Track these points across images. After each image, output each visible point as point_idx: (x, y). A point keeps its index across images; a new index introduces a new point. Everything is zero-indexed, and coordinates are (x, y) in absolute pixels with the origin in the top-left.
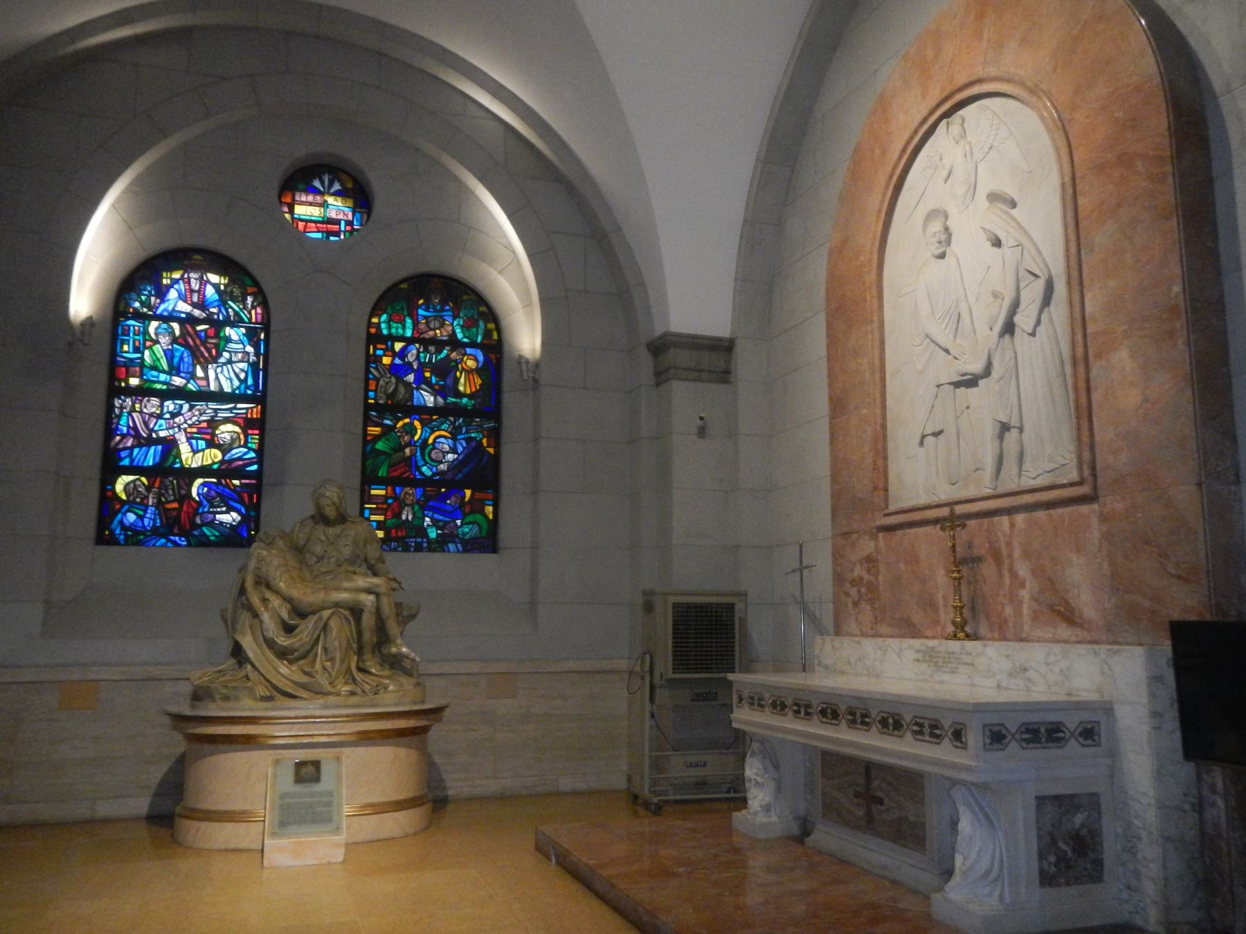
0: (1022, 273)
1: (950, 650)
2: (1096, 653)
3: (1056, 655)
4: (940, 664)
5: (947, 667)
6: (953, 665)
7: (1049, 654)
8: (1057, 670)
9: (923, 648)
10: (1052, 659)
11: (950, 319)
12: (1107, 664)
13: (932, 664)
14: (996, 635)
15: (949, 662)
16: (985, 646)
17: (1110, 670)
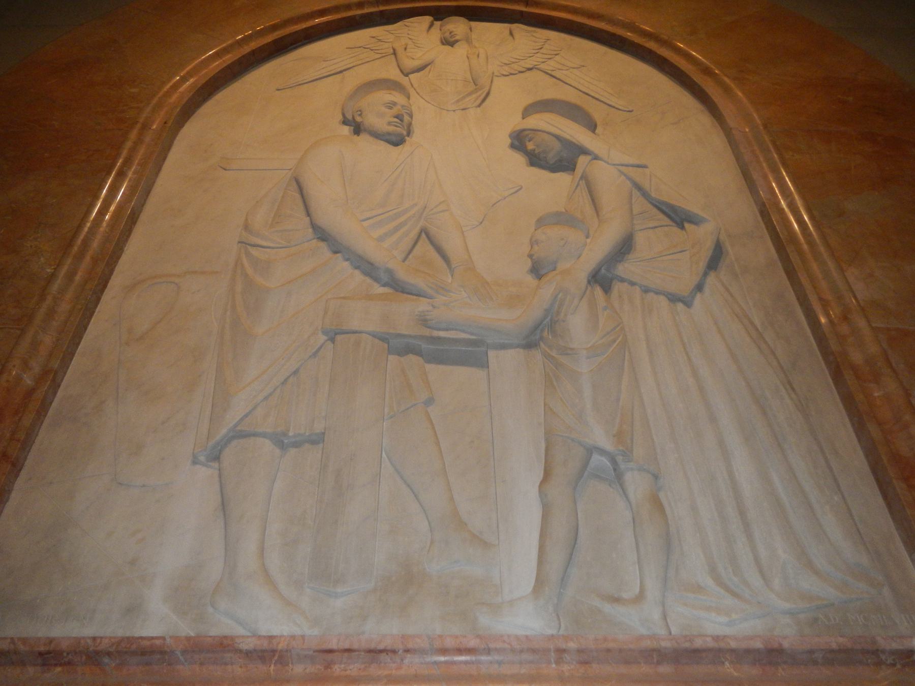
0: (639, 204)
11: (396, 229)
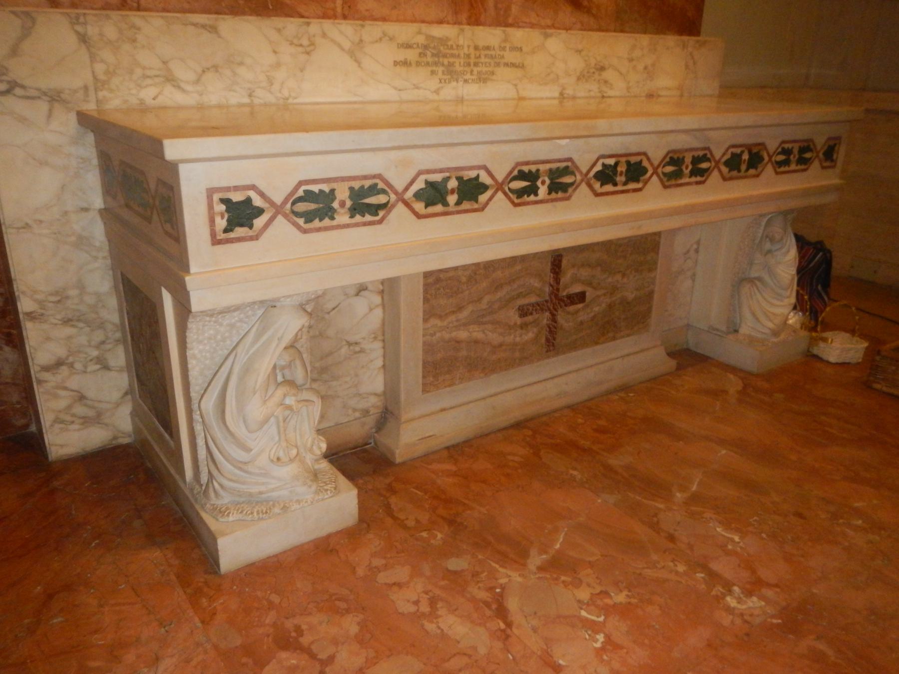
1: (481, 44)
2: (684, 46)
3: (642, 49)
4: (458, 68)
5: (472, 72)
6: (484, 69)
7: (633, 47)
8: (640, 67)
9: (421, 39)
10: (637, 53)
12: (693, 58)
13: (440, 69)
14: (463, 17)
15: (476, 64)
16: (547, 36)
17: (695, 63)
